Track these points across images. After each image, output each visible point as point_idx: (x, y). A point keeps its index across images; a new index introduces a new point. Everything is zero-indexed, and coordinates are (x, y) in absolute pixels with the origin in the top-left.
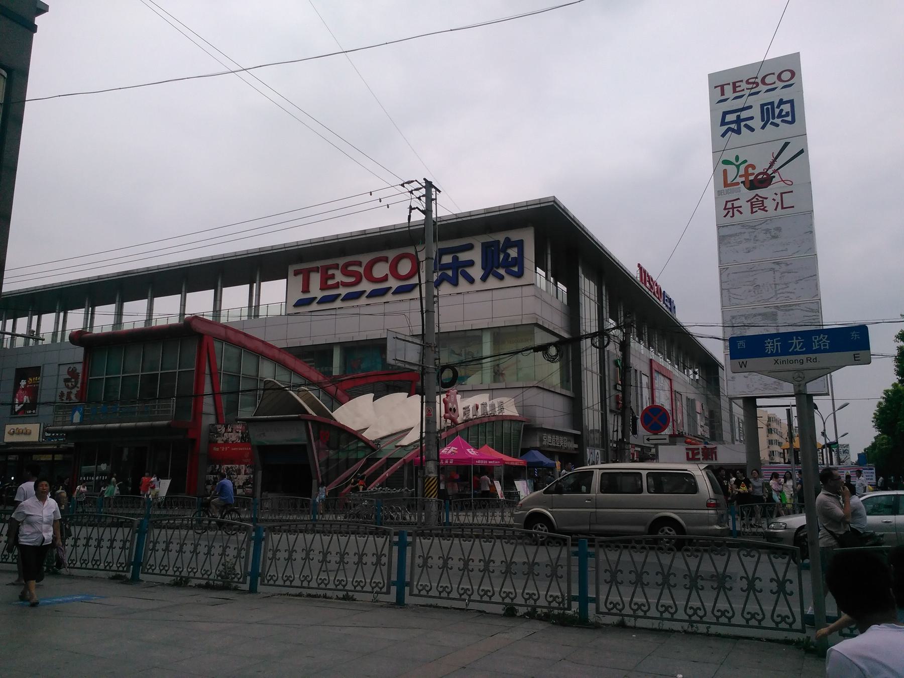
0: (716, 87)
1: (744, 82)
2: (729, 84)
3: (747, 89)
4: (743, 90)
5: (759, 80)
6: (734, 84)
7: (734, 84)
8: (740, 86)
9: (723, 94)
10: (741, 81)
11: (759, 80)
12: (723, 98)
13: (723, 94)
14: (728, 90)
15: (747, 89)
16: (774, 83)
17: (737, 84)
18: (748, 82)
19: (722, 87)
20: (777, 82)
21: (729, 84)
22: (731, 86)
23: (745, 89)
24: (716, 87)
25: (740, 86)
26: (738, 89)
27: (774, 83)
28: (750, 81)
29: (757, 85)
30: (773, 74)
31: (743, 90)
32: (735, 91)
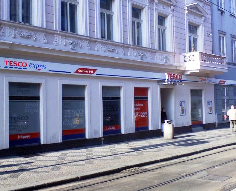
0: (5, 61)
1: (13, 62)
2: (8, 61)
5: (17, 63)
6: (10, 62)
9: (7, 65)
11: (17, 63)
13: (7, 65)
16: (21, 66)
17: (11, 62)
18: (14, 63)
19: (7, 62)
21: (8, 61)
24: (5, 61)
26: (11, 64)
27: (21, 66)
28: (15, 63)
29: (17, 65)
30: (21, 63)
32: (10, 65)
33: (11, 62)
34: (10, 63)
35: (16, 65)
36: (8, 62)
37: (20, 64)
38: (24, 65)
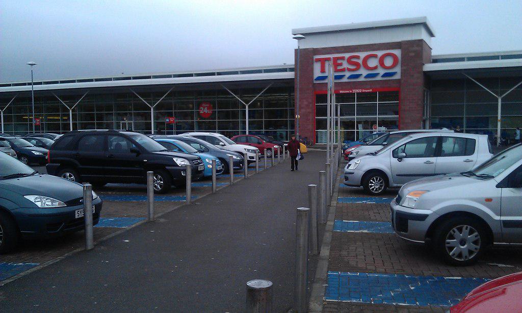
3: (349, 70)
4: (343, 70)
5: (360, 61)
8: (341, 64)
11: (360, 61)
15: (349, 70)
17: (339, 62)
21: (328, 59)
22: (332, 62)
23: (346, 69)
25: (341, 64)
26: (339, 68)
27: (376, 68)
31: (343, 70)
32: (336, 71)
33: (339, 62)
36: (327, 64)
37: (373, 63)
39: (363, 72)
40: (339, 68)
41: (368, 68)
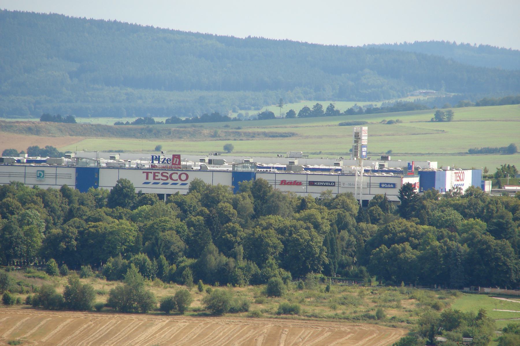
1: (160, 173)
2: (151, 173)
3: (162, 179)
4: (159, 179)
5: (168, 175)
6: (154, 173)
7: (154, 173)
8: (157, 176)
9: (147, 178)
10: (159, 173)
11: (168, 175)
12: (147, 181)
13: (147, 178)
14: (151, 176)
15: (162, 179)
16: (177, 180)
17: (156, 174)
18: (162, 175)
20: (178, 179)
24: (144, 172)
25: (157, 176)
26: (156, 178)
27: (177, 180)
28: (164, 174)
31: (159, 179)
32: (154, 179)
33: (156, 174)
34: (154, 176)
35: (166, 178)
36: (149, 174)
38: (183, 177)
39: (169, 180)
40: (156, 178)
41: (171, 179)
